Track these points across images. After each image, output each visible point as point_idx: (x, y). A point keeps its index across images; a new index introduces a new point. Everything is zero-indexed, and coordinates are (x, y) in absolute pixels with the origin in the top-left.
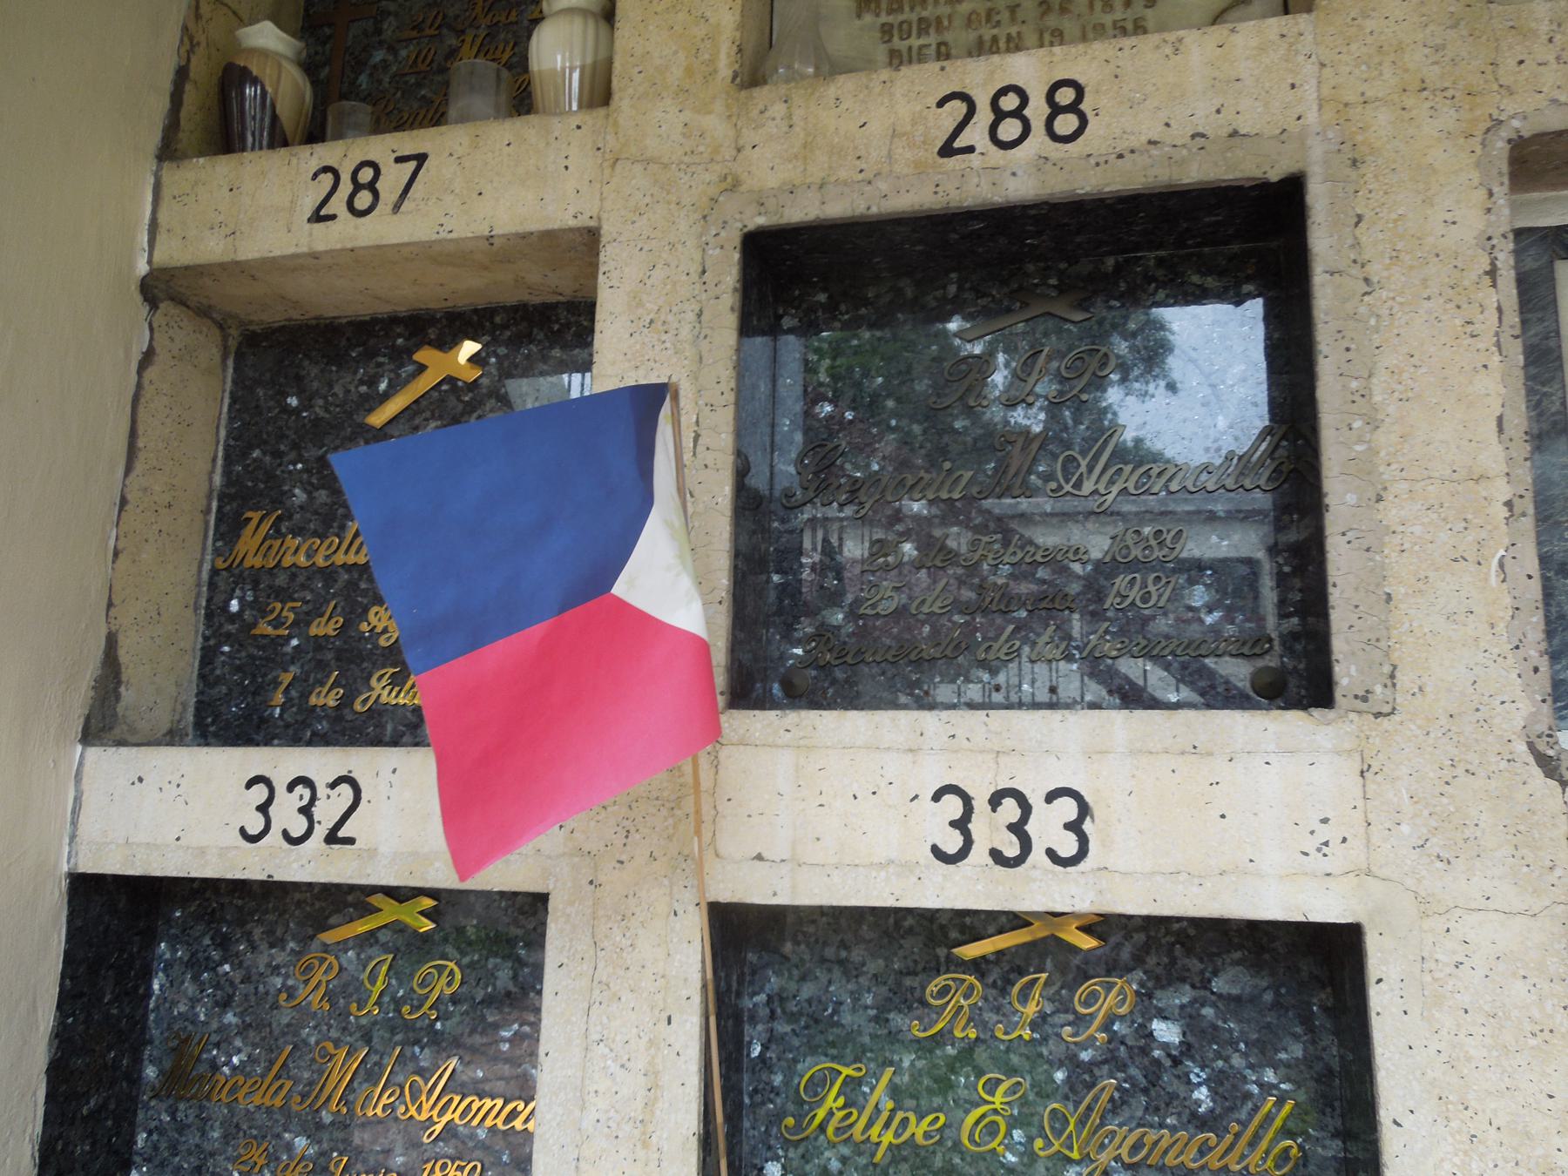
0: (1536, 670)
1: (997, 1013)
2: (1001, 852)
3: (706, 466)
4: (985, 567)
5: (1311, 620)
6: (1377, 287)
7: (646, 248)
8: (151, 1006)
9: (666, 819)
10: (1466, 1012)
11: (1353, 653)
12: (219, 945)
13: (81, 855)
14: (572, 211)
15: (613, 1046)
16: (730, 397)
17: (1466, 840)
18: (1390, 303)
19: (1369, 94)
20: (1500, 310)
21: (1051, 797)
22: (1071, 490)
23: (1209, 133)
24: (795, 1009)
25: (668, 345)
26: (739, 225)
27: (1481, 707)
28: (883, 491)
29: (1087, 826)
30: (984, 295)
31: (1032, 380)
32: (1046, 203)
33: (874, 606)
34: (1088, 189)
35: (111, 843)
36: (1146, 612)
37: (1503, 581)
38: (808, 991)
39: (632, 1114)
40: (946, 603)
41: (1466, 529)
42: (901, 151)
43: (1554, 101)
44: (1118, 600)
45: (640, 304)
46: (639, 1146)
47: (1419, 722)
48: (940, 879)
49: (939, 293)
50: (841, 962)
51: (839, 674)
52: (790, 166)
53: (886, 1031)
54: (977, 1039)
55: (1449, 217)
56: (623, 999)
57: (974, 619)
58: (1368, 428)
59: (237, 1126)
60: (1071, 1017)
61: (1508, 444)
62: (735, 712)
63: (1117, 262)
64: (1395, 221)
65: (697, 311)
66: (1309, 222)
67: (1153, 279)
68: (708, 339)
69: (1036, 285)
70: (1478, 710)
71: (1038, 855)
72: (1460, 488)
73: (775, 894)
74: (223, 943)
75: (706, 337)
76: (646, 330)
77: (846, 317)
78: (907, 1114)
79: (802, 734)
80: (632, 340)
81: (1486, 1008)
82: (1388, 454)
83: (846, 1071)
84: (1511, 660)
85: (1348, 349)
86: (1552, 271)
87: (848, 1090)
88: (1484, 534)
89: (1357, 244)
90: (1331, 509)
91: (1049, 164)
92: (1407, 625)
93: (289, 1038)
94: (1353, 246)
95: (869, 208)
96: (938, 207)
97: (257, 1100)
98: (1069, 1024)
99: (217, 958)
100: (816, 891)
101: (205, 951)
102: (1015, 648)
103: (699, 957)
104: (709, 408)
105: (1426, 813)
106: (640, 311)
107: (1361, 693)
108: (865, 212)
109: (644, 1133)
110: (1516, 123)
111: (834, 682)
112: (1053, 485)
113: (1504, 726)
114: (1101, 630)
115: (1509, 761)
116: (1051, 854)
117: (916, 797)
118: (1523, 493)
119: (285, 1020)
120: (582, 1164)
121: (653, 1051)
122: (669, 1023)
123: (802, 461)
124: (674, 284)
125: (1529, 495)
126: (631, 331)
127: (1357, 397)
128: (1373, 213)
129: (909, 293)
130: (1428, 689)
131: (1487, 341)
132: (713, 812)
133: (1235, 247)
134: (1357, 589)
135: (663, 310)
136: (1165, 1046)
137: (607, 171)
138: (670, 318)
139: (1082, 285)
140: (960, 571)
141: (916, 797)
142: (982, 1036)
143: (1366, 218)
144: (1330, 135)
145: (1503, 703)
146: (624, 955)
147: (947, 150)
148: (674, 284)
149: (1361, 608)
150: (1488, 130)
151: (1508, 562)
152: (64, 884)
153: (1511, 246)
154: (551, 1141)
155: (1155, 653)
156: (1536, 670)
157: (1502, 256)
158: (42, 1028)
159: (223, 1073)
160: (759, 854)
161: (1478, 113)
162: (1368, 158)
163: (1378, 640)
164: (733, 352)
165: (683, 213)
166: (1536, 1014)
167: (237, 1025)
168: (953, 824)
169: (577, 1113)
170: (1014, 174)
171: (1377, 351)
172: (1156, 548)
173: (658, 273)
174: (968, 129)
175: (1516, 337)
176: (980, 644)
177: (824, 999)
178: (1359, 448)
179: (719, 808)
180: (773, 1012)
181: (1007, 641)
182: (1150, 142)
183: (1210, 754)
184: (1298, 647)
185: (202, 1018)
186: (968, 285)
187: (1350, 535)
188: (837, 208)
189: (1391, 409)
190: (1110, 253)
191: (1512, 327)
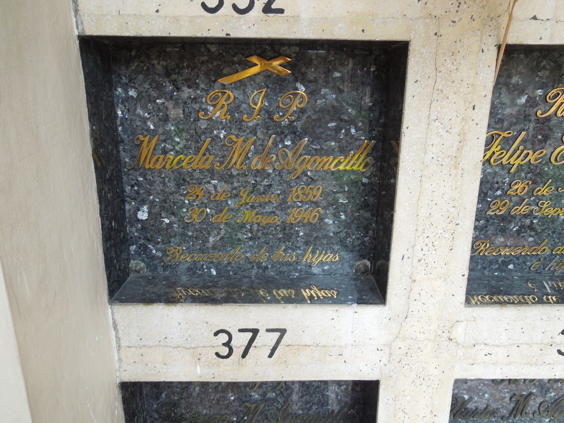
8: (118, 123)
12: (155, 88)
13: (85, 24)
15: (442, 122)
35: (106, 15)
39: (451, 154)
46: (453, 168)
56: (450, 98)
59: (184, 179)
73: (541, 38)
74: (159, 87)
78: (528, 151)
83: (505, 134)
87: (502, 143)
93: (208, 135)
97: (194, 165)
99: (155, 95)
101: (146, 92)
109: (456, 162)
119: (203, 127)
120: (423, 179)
121: (463, 123)
122: (474, 109)
146: (452, 74)
152: (78, 42)
154: (408, 169)
159: (171, 155)
167: (175, 131)
169: (422, 155)
185: (152, 127)
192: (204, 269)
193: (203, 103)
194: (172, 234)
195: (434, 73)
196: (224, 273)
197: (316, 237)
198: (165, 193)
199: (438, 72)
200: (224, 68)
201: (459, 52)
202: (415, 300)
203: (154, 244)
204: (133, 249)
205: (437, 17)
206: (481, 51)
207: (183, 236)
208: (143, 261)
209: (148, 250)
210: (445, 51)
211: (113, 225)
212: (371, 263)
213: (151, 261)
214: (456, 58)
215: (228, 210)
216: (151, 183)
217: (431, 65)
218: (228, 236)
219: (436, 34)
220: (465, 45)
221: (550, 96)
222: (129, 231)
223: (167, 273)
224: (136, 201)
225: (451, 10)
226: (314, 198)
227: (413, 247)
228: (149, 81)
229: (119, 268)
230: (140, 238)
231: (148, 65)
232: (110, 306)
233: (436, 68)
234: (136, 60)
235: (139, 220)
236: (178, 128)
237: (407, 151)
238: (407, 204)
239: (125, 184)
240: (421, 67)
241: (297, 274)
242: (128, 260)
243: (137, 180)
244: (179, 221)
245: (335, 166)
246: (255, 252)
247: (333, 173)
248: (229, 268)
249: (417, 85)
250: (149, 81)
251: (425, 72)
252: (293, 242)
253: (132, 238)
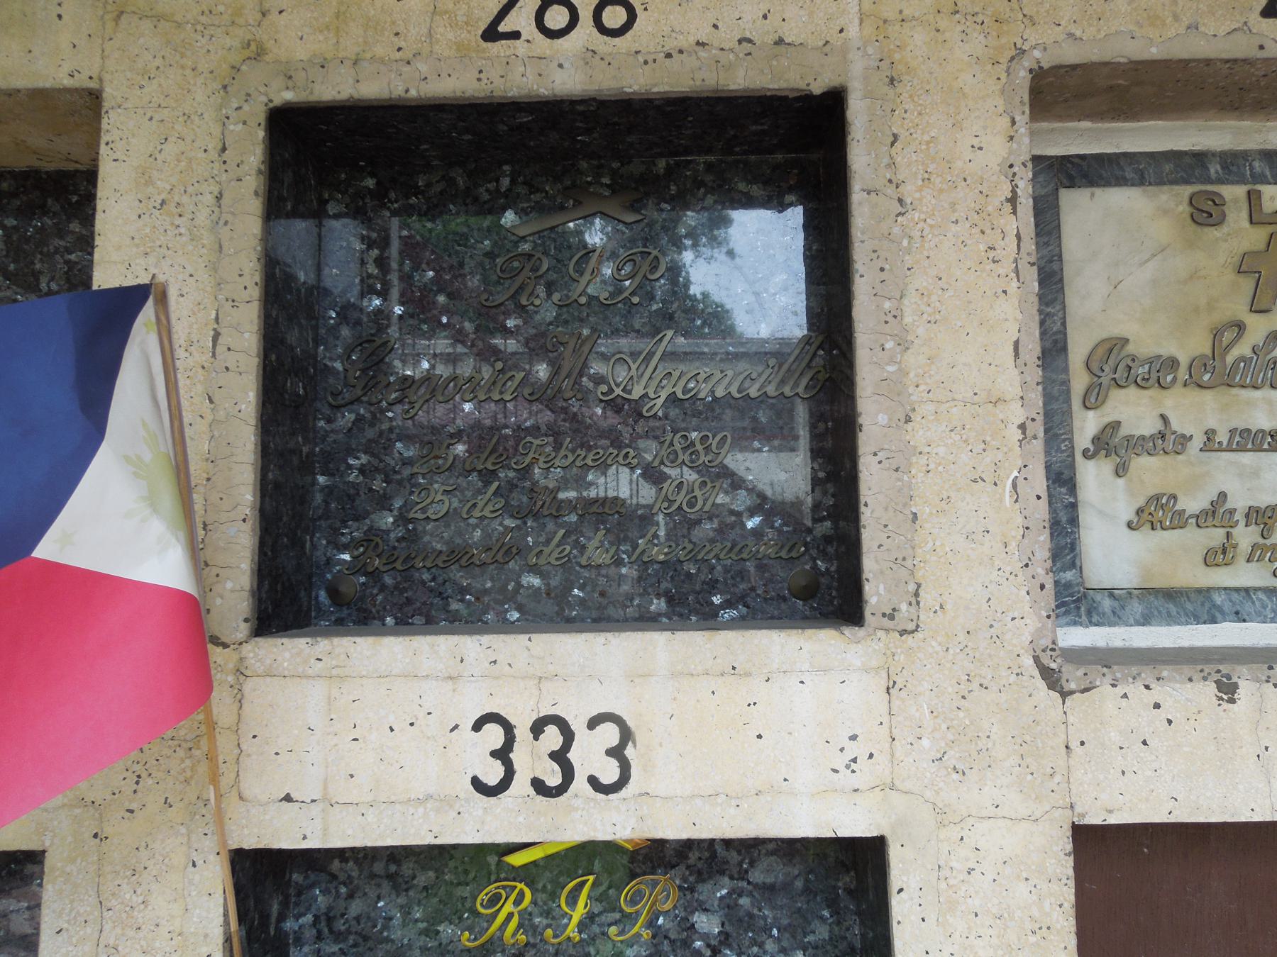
0: (1042, 587)
1: (547, 918)
2: (543, 782)
3: (227, 368)
4: (537, 471)
5: (842, 524)
6: (909, 207)
7: (157, 117)
9: (183, 761)
10: (976, 915)
11: (882, 572)
14: (67, 68)
16: (255, 293)
17: (979, 752)
18: (921, 224)
19: (906, 12)
20: (1018, 237)
21: (593, 723)
22: (621, 393)
23: (755, 39)
24: (343, 928)
25: (183, 230)
26: (265, 99)
27: (993, 623)
28: (434, 390)
29: (629, 752)
30: (538, 190)
31: (584, 281)
32: (594, 99)
33: (424, 510)
34: (636, 88)
36: (692, 517)
37: (1016, 501)
38: (356, 908)
40: (497, 507)
41: (984, 450)
42: (441, 30)
43: (1070, 35)
44: (666, 504)
45: (150, 182)
47: (939, 639)
48: (480, 812)
49: (492, 186)
50: (391, 877)
51: (388, 580)
52: (321, 38)
53: (436, 943)
54: (527, 944)
55: (976, 142)
57: (525, 523)
58: (898, 349)
60: (617, 916)
61: (1023, 369)
62: (260, 640)
63: (668, 164)
64: (928, 143)
65: (216, 193)
66: (849, 138)
67: (701, 184)
68: (229, 227)
69: (590, 183)
70: (991, 626)
71: (580, 783)
72: (980, 410)
73: (305, 838)
75: (226, 223)
76: (157, 213)
77: (396, 205)
79: (334, 663)
80: (141, 222)
81: (994, 911)
82: (917, 376)
84: (1021, 578)
85: (882, 270)
86: (1057, 198)
88: (1000, 456)
89: (892, 164)
90: (864, 428)
91: (597, 57)
92: (931, 544)
94: (888, 166)
95: (407, 91)
96: (482, 95)
98: (615, 923)
100: (350, 832)
102: (565, 553)
103: (221, 910)
104: (230, 303)
105: (944, 727)
106: (150, 189)
107: (888, 611)
108: (403, 94)
110: (1037, 54)
111: (383, 588)
112: (604, 388)
113: (1014, 641)
114: (649, 536)
115: (1017, 674)
116: (593, 781)
117: (456, 727)
118: (1035, 416)
123: (349, 357)
124: (190, 160)
125: (1040, 418)
126: (140, 212)
127: (889, 318)
128: (908, 133)
129: (461, 182)
130: (948, 607)
131: (1007, 267)
132: (237, 751)
133: (779, 157)
134: (886, 509)
135: (176, 190)
136: (705, 937)
137: (110, 25)
138: (185, 199)
139: (633, 185)
140: (511, 474)
141: (456, 727)
142: (532, 941)
143: (901, 138)
144: (870, 51)
145: (1013, 619)
146: (136, 913)
147: (491, 34)
148: (190, 160)
149: (890, 527)
150: (1012, 58)
151: (1020, 482)
153: (1030, 175)
155: (700, 557)
156: (1042, 587)
157: (1021, 184)
160: (288, 795)
161: (1003, 41)
162: (905, 78)
163: (904, 559)
164: (257, 242)
165: (201, 80)
166: (1036, 913)
168: (494, 754)
170: (561, 66)
171: (908, 273)
172: (702, 453)
173: (171, 148)
174: (513, 13)
175: (1032, 264)
176: (531, 549)
177: (373, 915)
178: (891, 368)
179: (244, 747)
180: (319, 932)
181: (558, 546)
182: (698, 43)
183: (748, 674)
184: (831, 550)
186: (521, 179)
187: (881, 455)
188: (373, 88)
189: (920, 331)
190: (661, 155)
191: (1028, 254)
195: (96, 913)
199: (104, 910)
201: (145, 868)
205: (97, 804)
206: (191, 864)
210: (118, 868)
214: (140, 880)
219: (96, 836)
220: (157, 856)
221: (483, 900)
225: (123, 789)
233: (101, 903)
240: (67, 902)
249: (60, 939)
251: (78, 912)
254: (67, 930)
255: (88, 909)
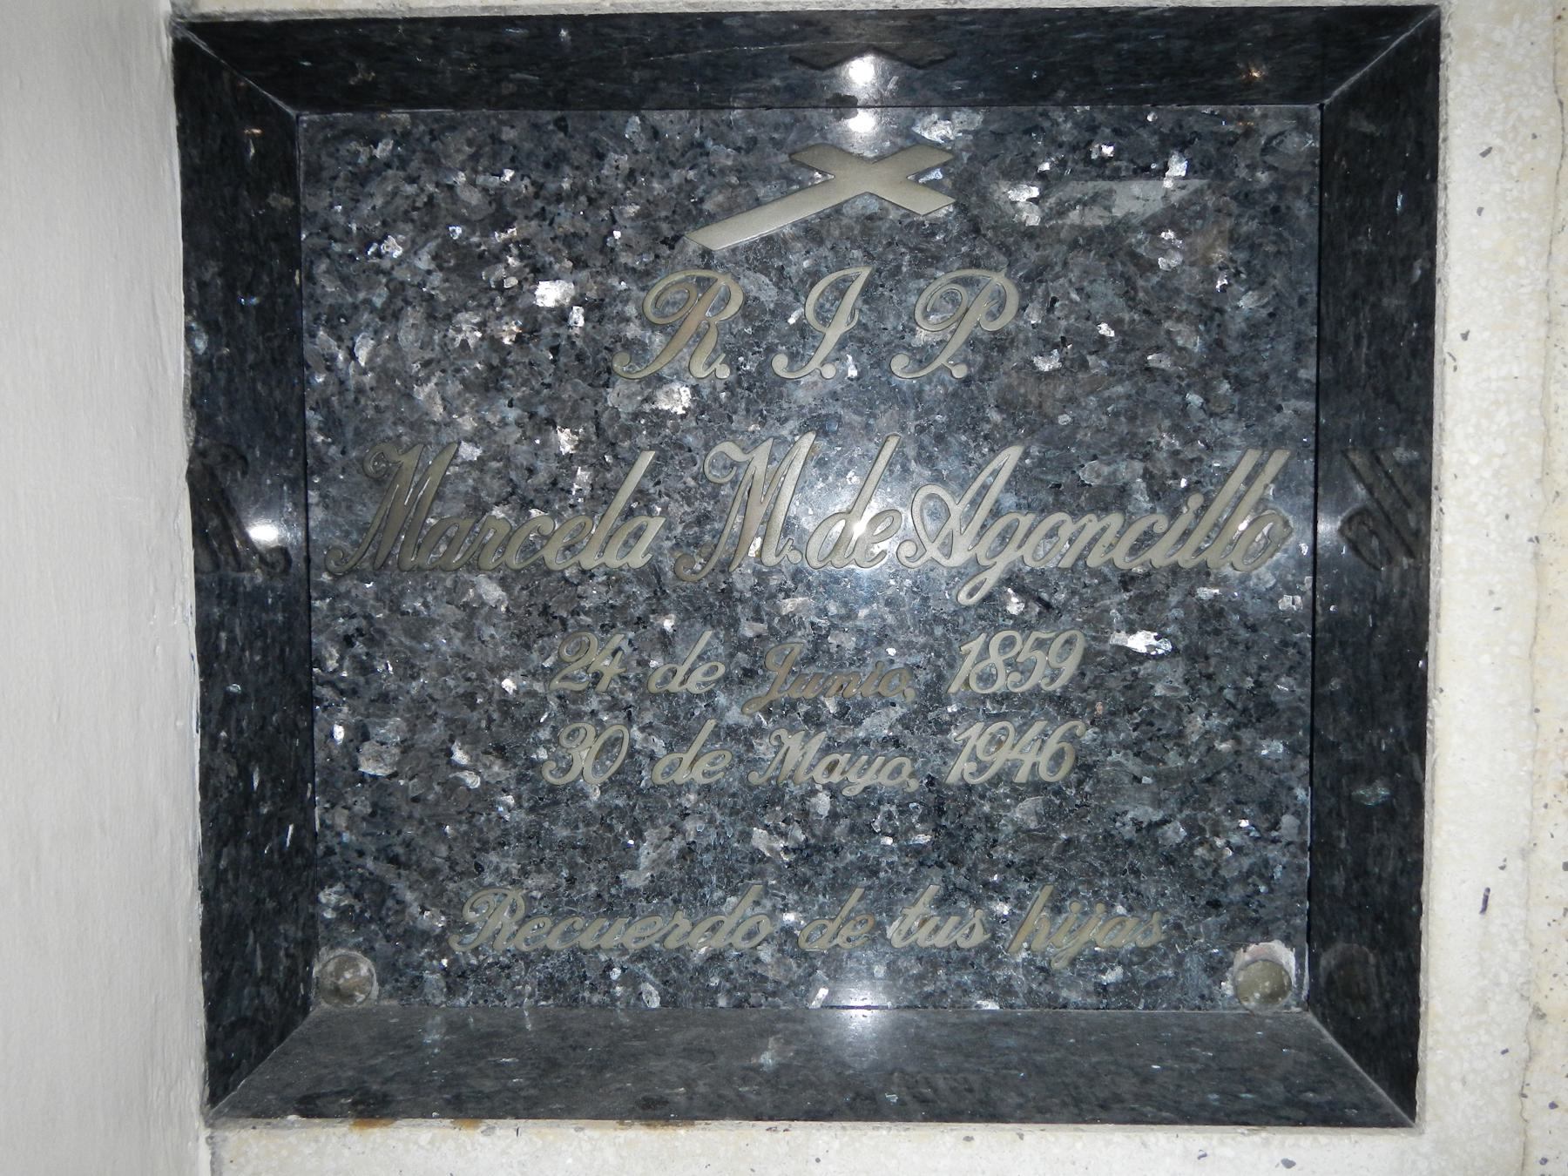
59: (545, 611)
120: (1547, 549)
154: (1481, 508)
158: (171, 373)
192: (611, 985)
193: (628, 320)
194: (492, 836)
195: (1553, 122)
196: (695, 1000)
197: (1069, 842)
198: (471, 668)
200: (707, 192)
202: (1553, 1106)
203: (415, 876)
204: (334, 898)
207: (532, 842)
208: (369, 951)
209: (390, 903)
211: (256, 784)
212: (1299, 956)
213: (399, 951)
215: (715, 734)
216: (419, 627)
217: (1541, 89)
218: (712, 838)
222: (323, 823)
223: (462, 1001)
224: (355, 702)
226: (1053, 680)
227: (1525, 854)
228: (432, 245)
229: (268, 969)
230: (361, 854)
231: (431, 188)
232: (208, 1132)
234: (390, 172)
235: (362, 778)
236: (532, 415)
237: (1471, 430)
238: (1486, 659)
239: (320, 632)
240: (1499, 98)
241: (991, 1005)
242: (308, 947)
243: (368, 617)
244: (521, 779)
245: (1135, 550)
246: (821, 907)
247: (1127, 580)
248: (715, 981)
250: (432, 245)
251: (1520, 118)
252: (975, 865)
253: (330, 851)
254: (1501, 150)
255: (1538, 113)
